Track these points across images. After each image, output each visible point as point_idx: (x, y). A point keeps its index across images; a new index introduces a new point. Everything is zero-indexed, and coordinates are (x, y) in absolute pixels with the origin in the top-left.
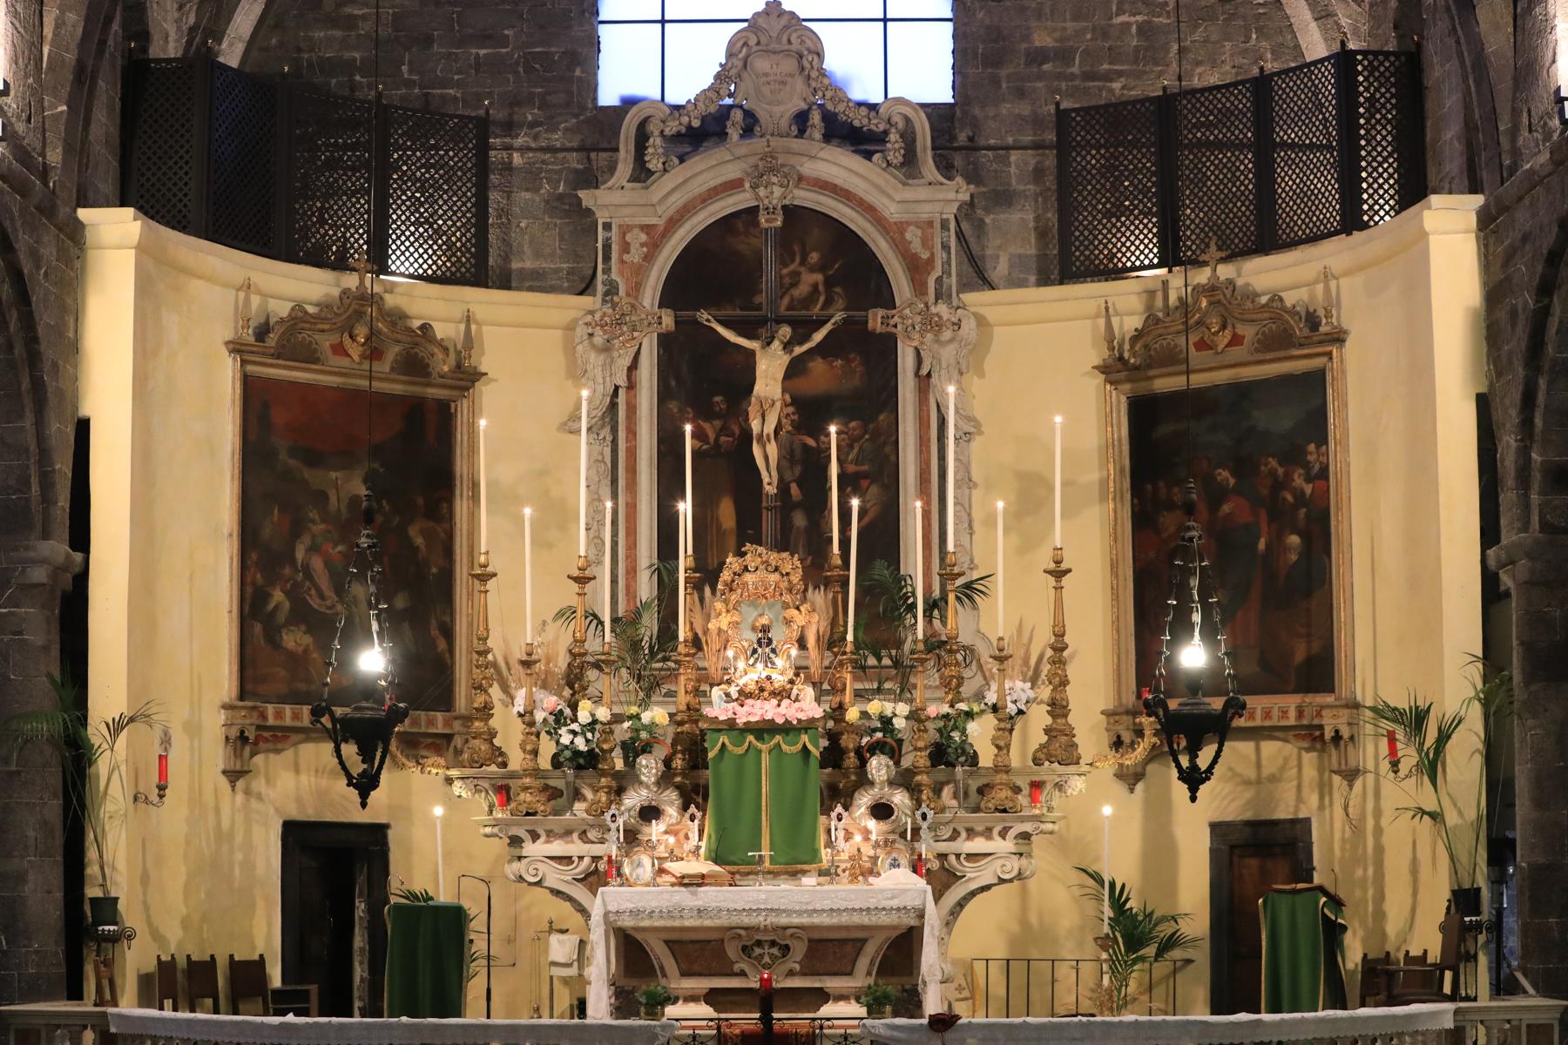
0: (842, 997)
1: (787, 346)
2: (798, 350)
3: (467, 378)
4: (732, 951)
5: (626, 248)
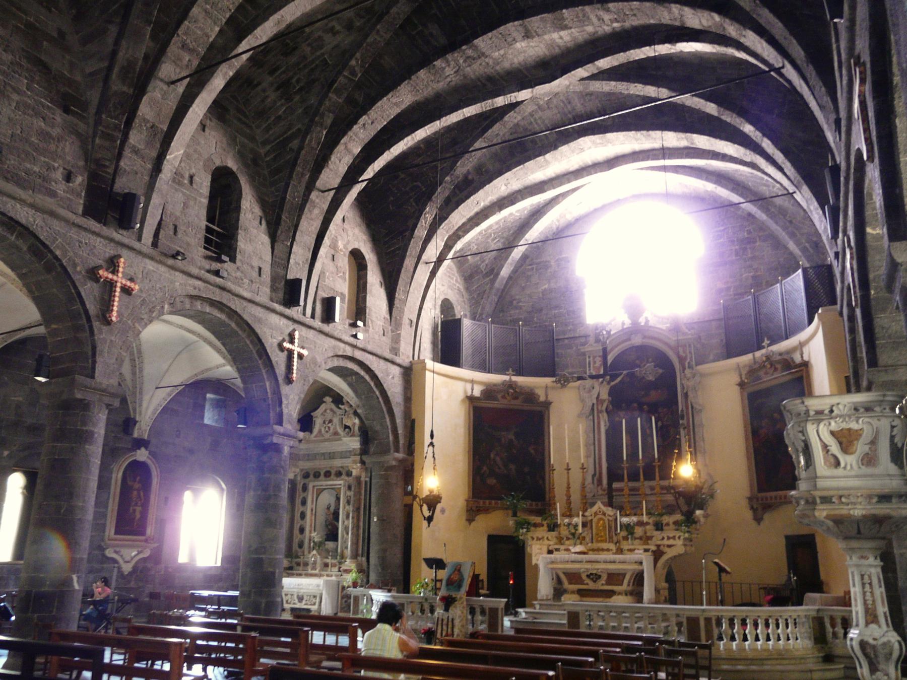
0: (620, 594)
1: (609, 383)
2: (612, 383)
3: (547, 404)
4: (584, 577)
5: (595, 363)
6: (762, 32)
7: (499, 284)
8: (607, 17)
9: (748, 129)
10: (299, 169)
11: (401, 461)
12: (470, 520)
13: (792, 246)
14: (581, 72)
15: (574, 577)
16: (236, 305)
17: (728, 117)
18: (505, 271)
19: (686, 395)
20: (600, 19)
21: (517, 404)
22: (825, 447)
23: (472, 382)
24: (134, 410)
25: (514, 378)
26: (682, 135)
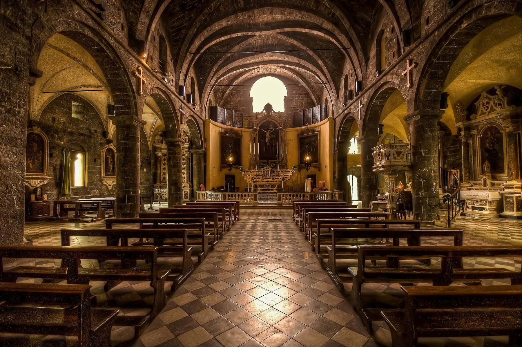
3: (242, 136)
6: (347, 35)
7: (225, 96)
8: (299, 15)
9: (320, 62)
10: (185, 42)
11: (203, 152)
12: (221, 170)
13: (313, 97)
14: (278, 31)
15: (261, 186)
16: (169, 92)
17: (316, 57)
18: (227, 92)
19: (281, 137)
20: (296, 15)
21: (233, 135)
22: (394, 155)
23: (221, 128)
24: (107, 128)
25: (233, 128)
26: (298, 59)
